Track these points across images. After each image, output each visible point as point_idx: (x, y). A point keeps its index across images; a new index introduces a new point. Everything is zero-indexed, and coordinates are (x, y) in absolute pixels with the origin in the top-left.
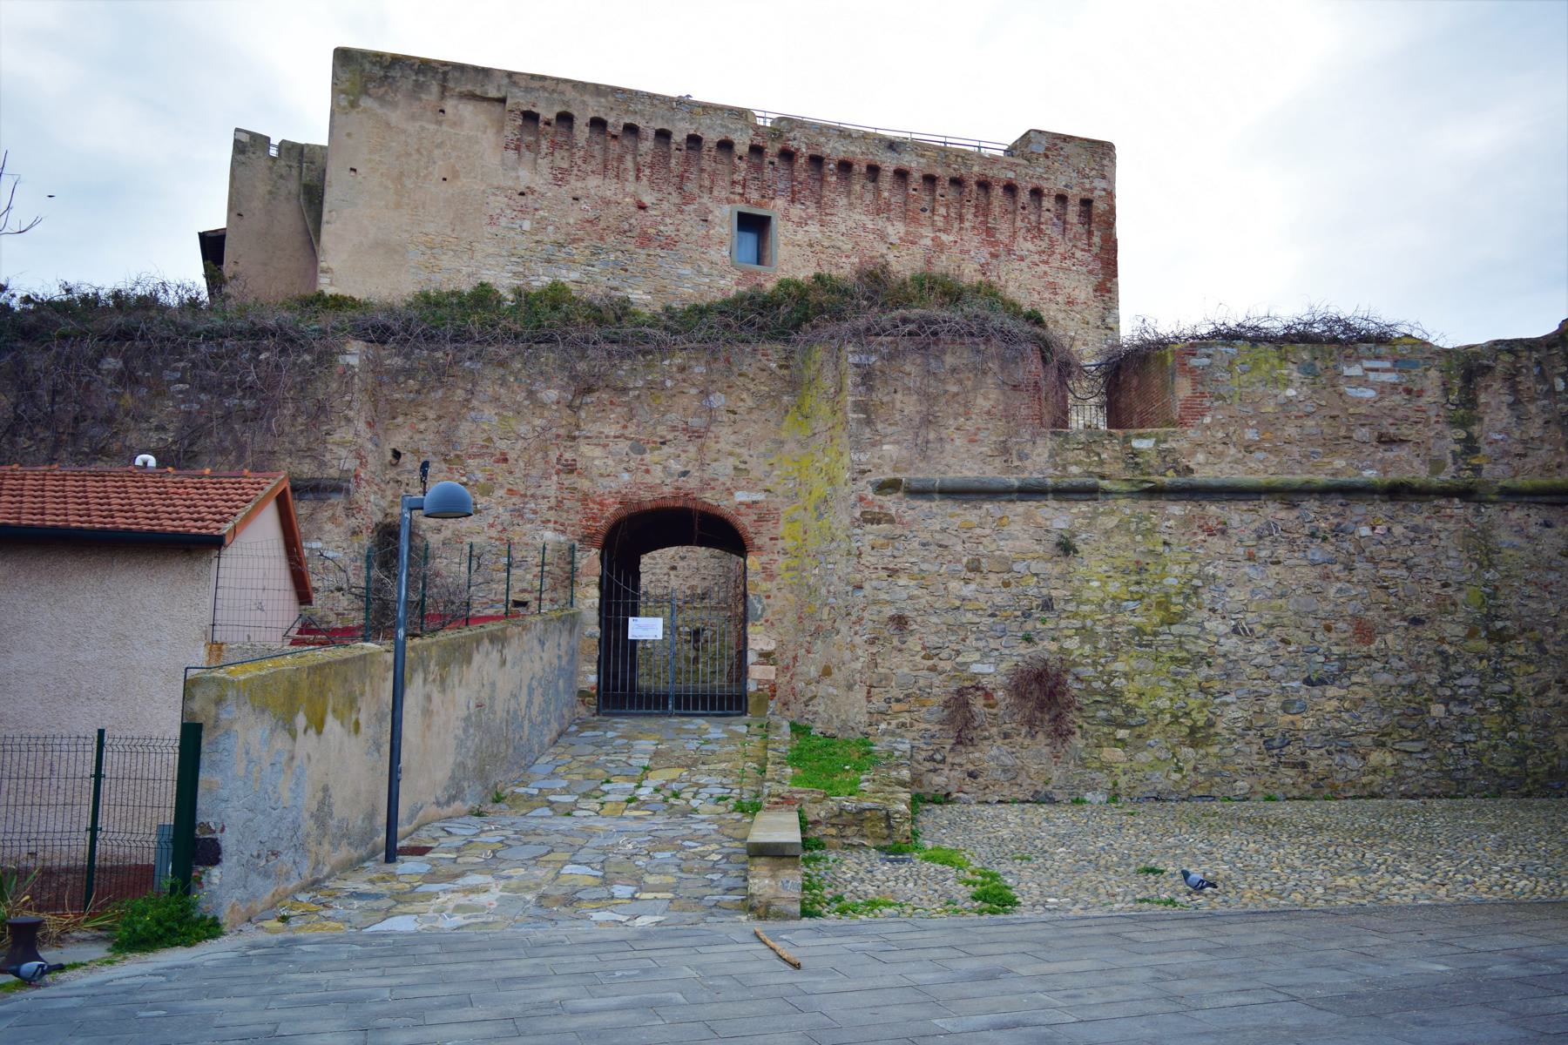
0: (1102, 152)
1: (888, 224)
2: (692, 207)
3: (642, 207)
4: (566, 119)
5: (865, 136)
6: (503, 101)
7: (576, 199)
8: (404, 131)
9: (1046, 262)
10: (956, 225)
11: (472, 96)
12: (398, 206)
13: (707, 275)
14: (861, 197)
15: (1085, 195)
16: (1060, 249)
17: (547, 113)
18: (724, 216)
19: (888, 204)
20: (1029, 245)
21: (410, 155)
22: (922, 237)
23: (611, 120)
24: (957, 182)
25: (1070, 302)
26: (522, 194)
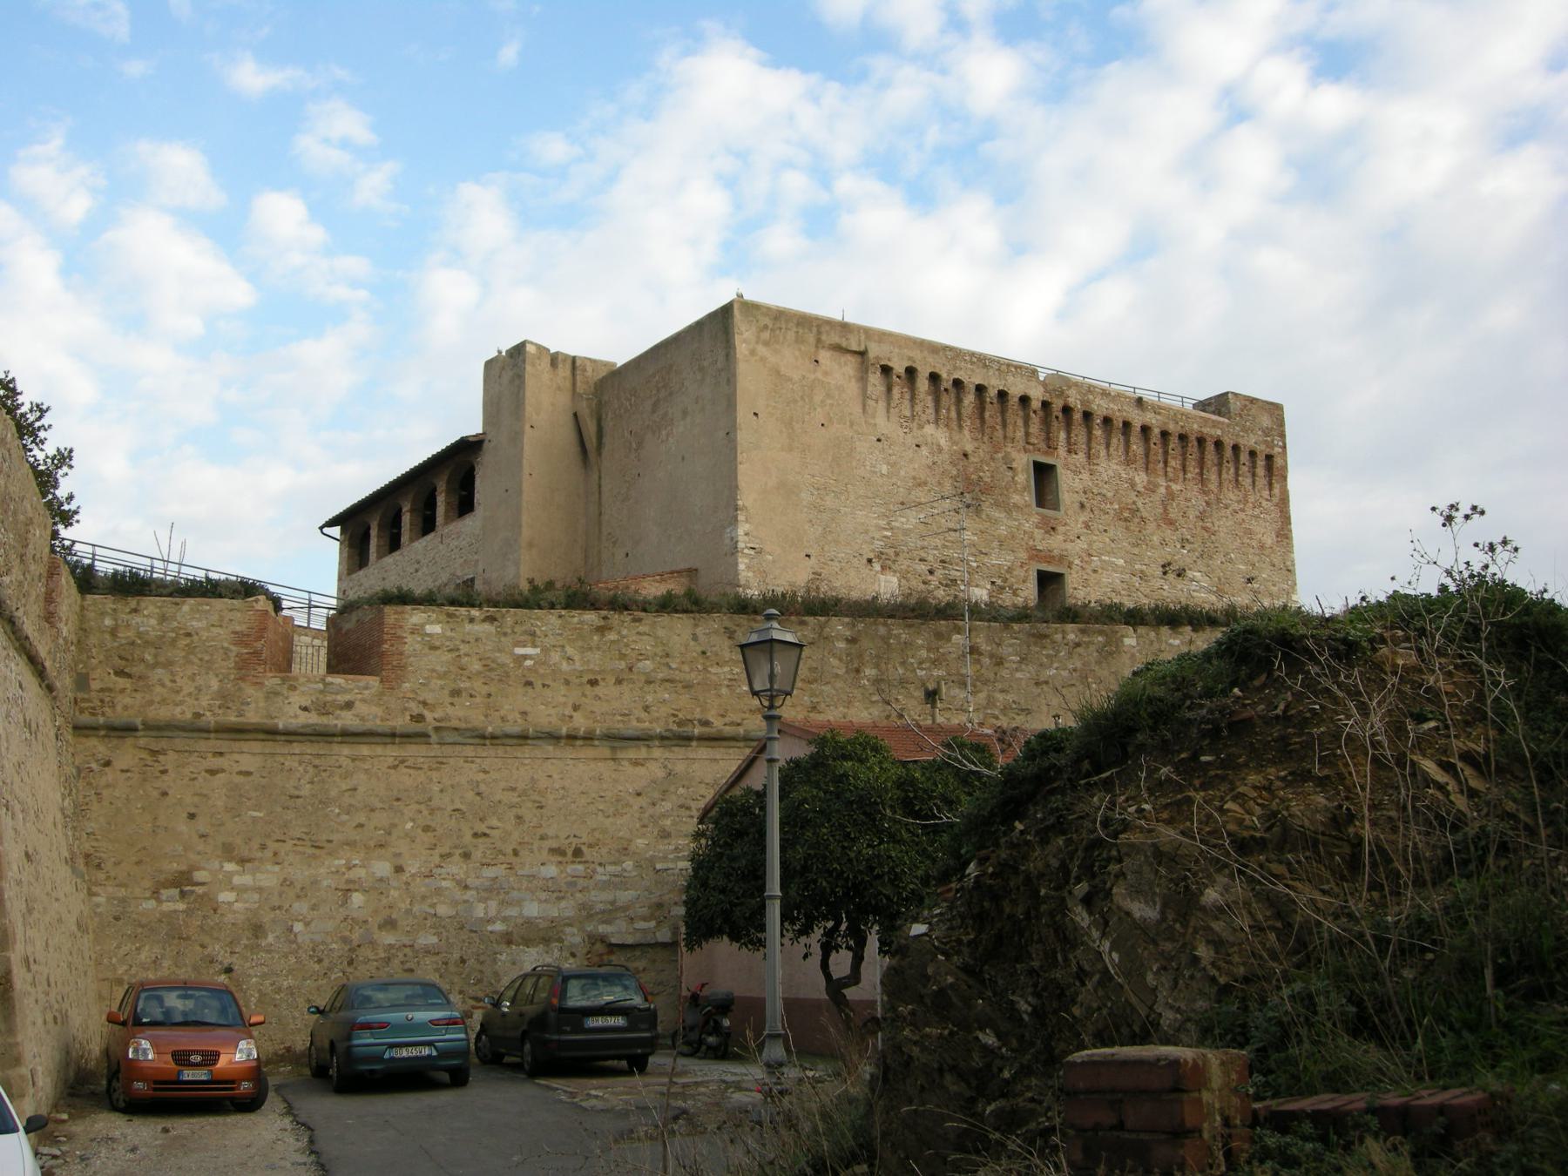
0: (1275, 410)
1: (1136, 473)
2: (1000, 455)
4: (911, 372)
5: (1119, 395)
6: (862, 354)
7: (917, 446)
8: (790, 379)
9: (1243, 510)
10: (1181, 475)
11: (839, 349)
12: (791, 449)
13: (1015, 520)
14: (1117, 450)
15: (1268, 451)
16: (1251, 499)
17: (899, 367)
18: (1023, 462)
20: (1231, 495)
21: (795, 401)
23: (944, 376)
24: (1183, 438)
25: (1262, 547)
26: (879, 440)
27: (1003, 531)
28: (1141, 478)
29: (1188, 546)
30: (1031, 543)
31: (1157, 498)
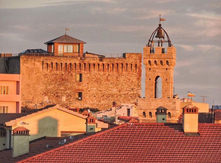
2: (70, 74)
3: (63, 75)
8: (29, 68)
9: (128, 75)
12: (29, 79)
14: (96, 69)
16: (131, 73)
19: (101, 69)
22: (106, 74)
25: (132, 82)
27: (69, 87)
28: (102, 73)
29: (112, 84)
30: (75, 88)
31: (105, 76)
